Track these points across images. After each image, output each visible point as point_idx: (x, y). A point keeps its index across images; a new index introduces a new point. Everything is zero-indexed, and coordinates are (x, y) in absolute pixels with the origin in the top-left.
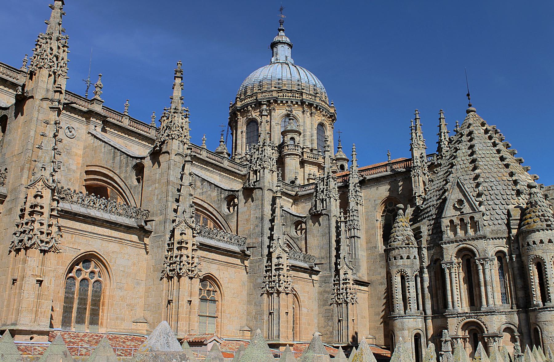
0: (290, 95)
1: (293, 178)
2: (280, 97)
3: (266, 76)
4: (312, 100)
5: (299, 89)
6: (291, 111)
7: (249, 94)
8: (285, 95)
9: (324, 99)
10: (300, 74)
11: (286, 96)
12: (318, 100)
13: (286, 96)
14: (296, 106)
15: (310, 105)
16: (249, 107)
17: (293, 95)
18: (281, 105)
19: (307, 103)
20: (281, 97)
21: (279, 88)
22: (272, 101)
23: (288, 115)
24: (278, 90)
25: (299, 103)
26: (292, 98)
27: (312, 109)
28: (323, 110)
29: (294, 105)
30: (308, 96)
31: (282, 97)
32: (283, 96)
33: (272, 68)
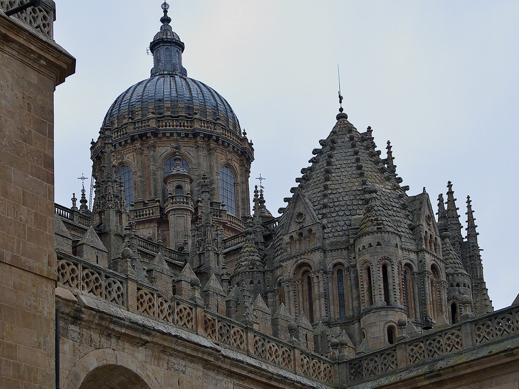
1: (182, 244)
3: (140, 97)
4: (209, 129)
5: (190, 114)
8: (168, 124)
10: (191, 91)
11: (170, 126)
12: (219, 131)
13: (170, 126)
15: (208, 137)
17: (180, 123)
20: (162, 127)
21: (160, 114)
26: (179, 128)
27: (210, 144)
28: (229, 144)
30: (203, 124)
32: (166, 126)
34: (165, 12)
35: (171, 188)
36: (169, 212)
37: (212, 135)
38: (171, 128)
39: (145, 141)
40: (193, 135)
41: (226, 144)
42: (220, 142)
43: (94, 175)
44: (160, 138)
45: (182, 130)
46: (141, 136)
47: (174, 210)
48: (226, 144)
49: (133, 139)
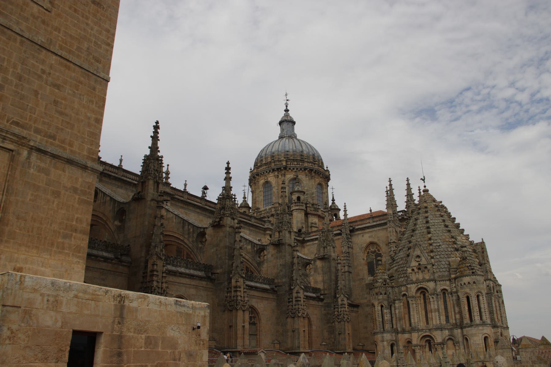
5: (302, 159)
6: (297, 176)
7: (264, 162)
9: (321, 165)
14: (301, 171)
15: (311, 170)
18: (290, 171)
22: (282, 169)
23: (294, 179)
25: (303, 169)
28: (320, 173)
29: (299, 171)
32: (291, 165)
33: (281, 142)
34: (287, 107)
35: (294, 197)
36: (293, 210)
38: (293, 165)
39: (280, 171)
40: (304, 169)
41: (319, 173)
42: (317, 173)
43: (250, 184)
44: (288, 170)
45: (299, 167)
46: (278, 169)
47: (296, 209)
48: (319, 173)
49: (273, 170)
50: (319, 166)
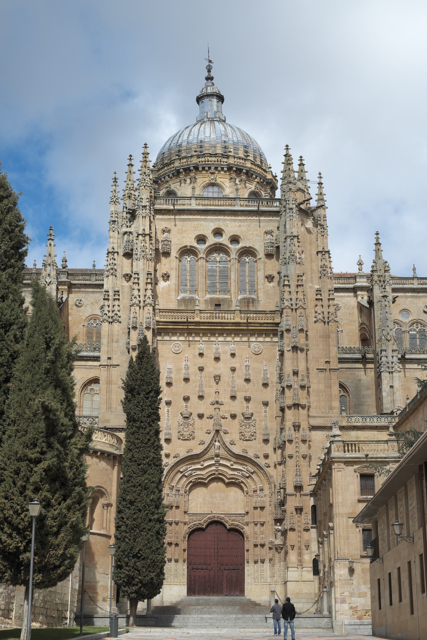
0: (213, 159)
2: (201, 163)
12: (249, 165)
14: (222, 172)
15: (239, 171)
16: (167, 177)
18: (204, 172)
19: (234, 169)
20: (202, 162)
21: (201, 152)
24: (199, 155)
25: (226, 169)
28: (256, 177)
31: (204, 163)
37: (243, 169)
40: (228, 168)
46: (185, 170)
50: (253, 163)
